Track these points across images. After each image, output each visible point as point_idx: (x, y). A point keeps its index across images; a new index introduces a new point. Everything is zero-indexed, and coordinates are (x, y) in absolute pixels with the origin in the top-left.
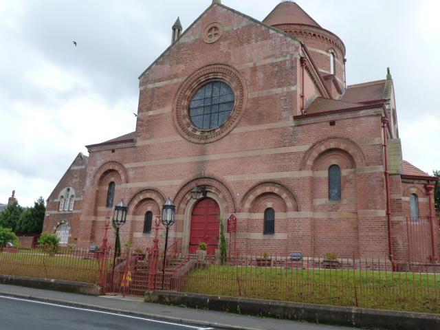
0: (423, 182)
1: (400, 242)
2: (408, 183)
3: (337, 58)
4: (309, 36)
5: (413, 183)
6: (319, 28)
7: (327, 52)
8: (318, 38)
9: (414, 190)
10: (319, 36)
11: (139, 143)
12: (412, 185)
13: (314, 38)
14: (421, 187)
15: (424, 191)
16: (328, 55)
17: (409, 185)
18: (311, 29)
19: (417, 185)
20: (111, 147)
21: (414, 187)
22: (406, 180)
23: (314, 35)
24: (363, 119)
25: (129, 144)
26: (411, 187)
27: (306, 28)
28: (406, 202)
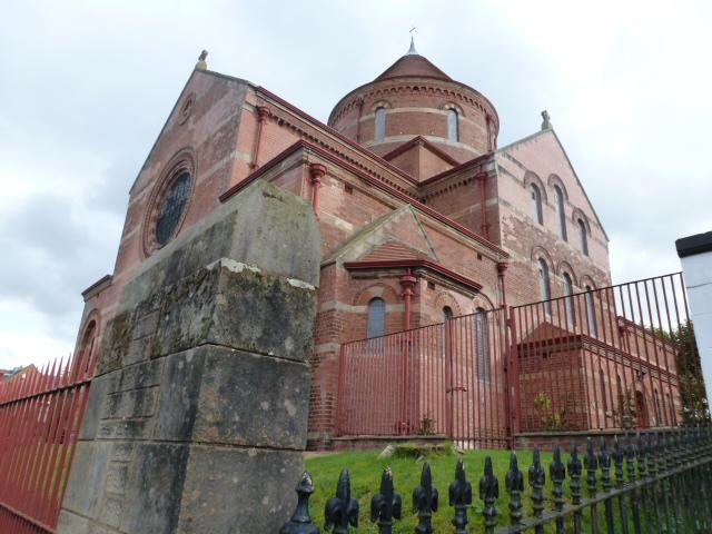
0: (397, 272)
1: (323, 395)
2: (365, 278)
3: (463, 115)
4: (408, 91)
5: (377, 278)
6: (447, 79)
7: (441, 108)
8: (423, 92)
9: (377, 291)
10: (424, 88)
11: (114, 281)
12: (376, 281)
13: (415, 92)
14: (394, 283)
15: (399, 290)
16: (443, 112)
17: (369, 282)
18: (410, 80)
19: (388, 282)
20: (95, 291)
21: (379, 285)
22: (359, 274)
23: (416, 88)
24: (285, 176)
25: (106, 284)
26: (372, 286)
27: (402, 81)
28: (359, 315)
